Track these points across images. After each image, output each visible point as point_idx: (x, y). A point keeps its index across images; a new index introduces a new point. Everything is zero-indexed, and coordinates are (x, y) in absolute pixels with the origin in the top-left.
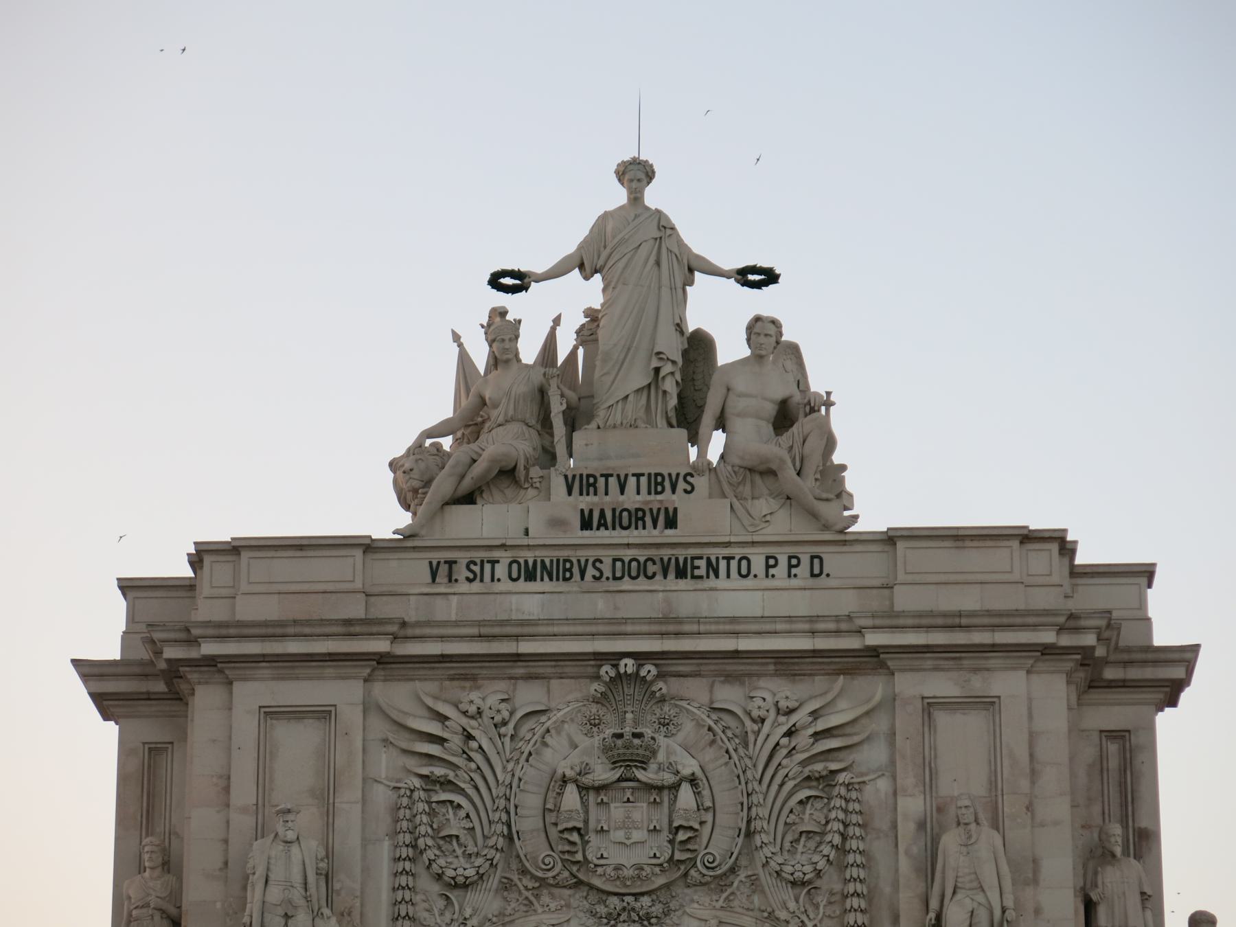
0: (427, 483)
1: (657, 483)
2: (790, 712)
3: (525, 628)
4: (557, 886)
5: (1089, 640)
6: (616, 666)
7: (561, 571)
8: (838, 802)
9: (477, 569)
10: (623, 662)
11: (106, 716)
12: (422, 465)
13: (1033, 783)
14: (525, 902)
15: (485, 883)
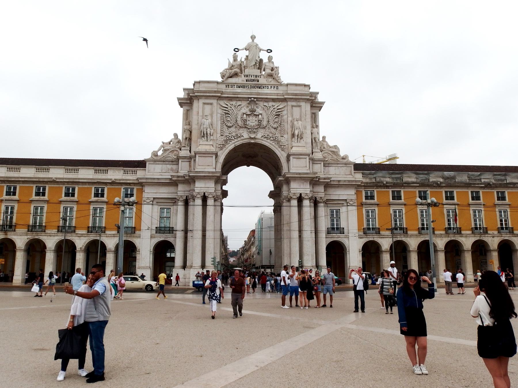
0: (226, 75)
1: (256, 76)
2: (274, 106)
3: (239, 93)
5: (314, 98)
6: (251, 99)
7: (243, 87)
9: (232, 86)
10: (252, 98)
11: (181, 107)
12: (224, 73)
13: (306, 117)
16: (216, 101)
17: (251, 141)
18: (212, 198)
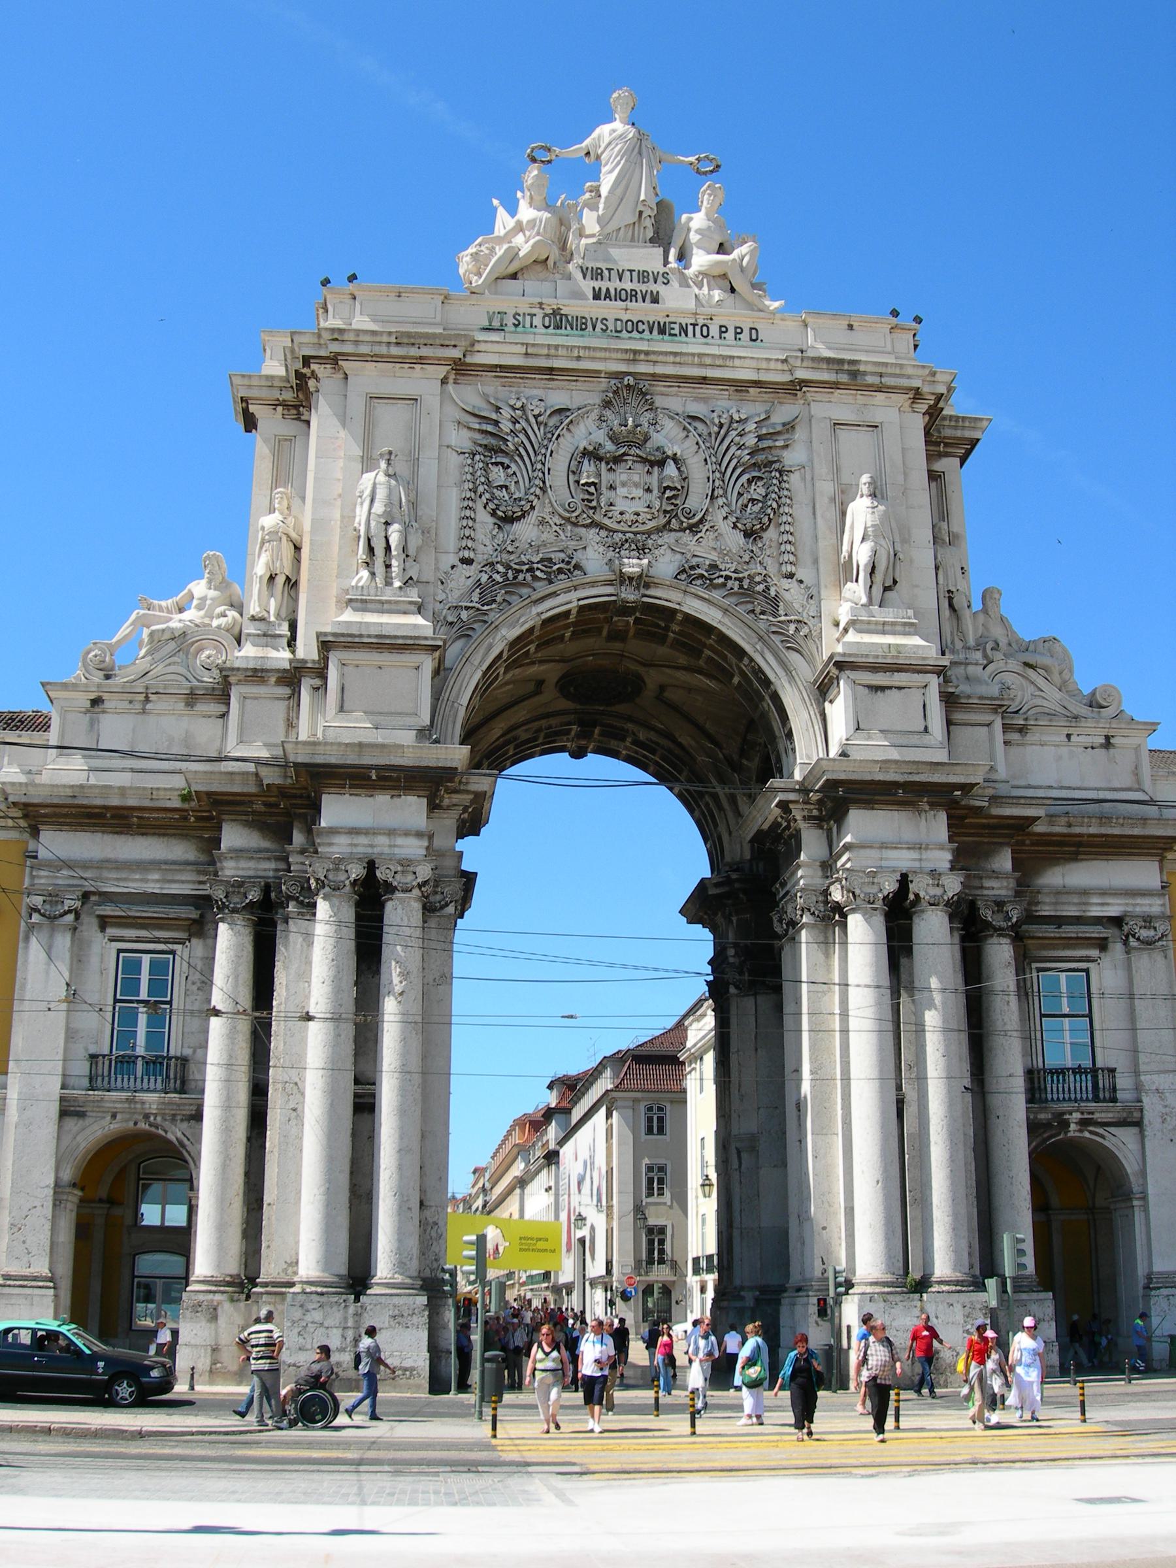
1: (643, 276)
4: (575, 524)
5: (942, 389)
8: (775, 481)
10: (626, 379)
17: (623, 595)
18: (416, 892)
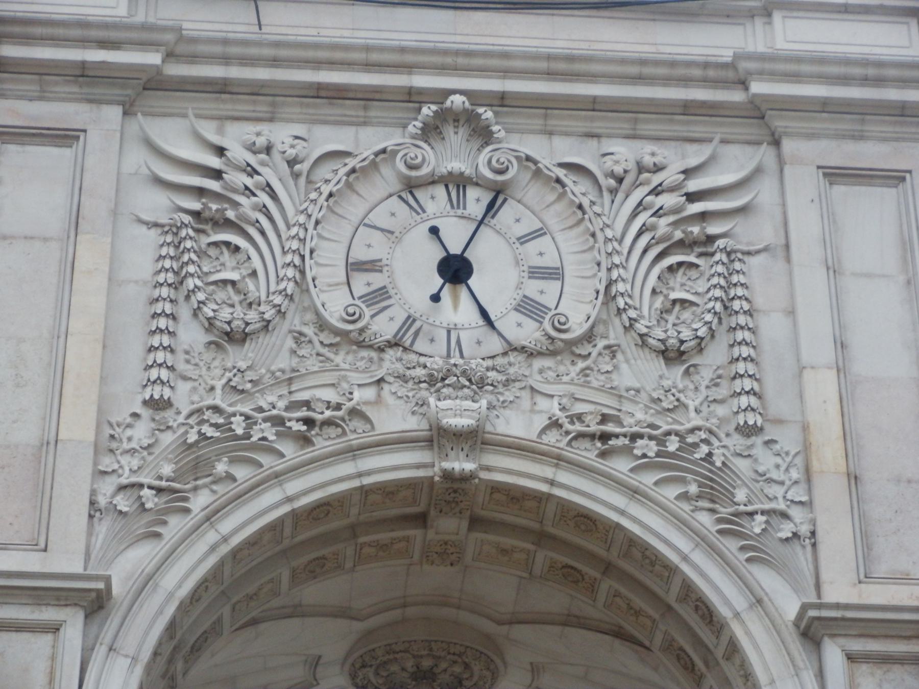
2: (658, 169)
8: (720, 269)
10: (452, 98)
14: (321, 358)
15: (268, 336)
16: (114, 113)
